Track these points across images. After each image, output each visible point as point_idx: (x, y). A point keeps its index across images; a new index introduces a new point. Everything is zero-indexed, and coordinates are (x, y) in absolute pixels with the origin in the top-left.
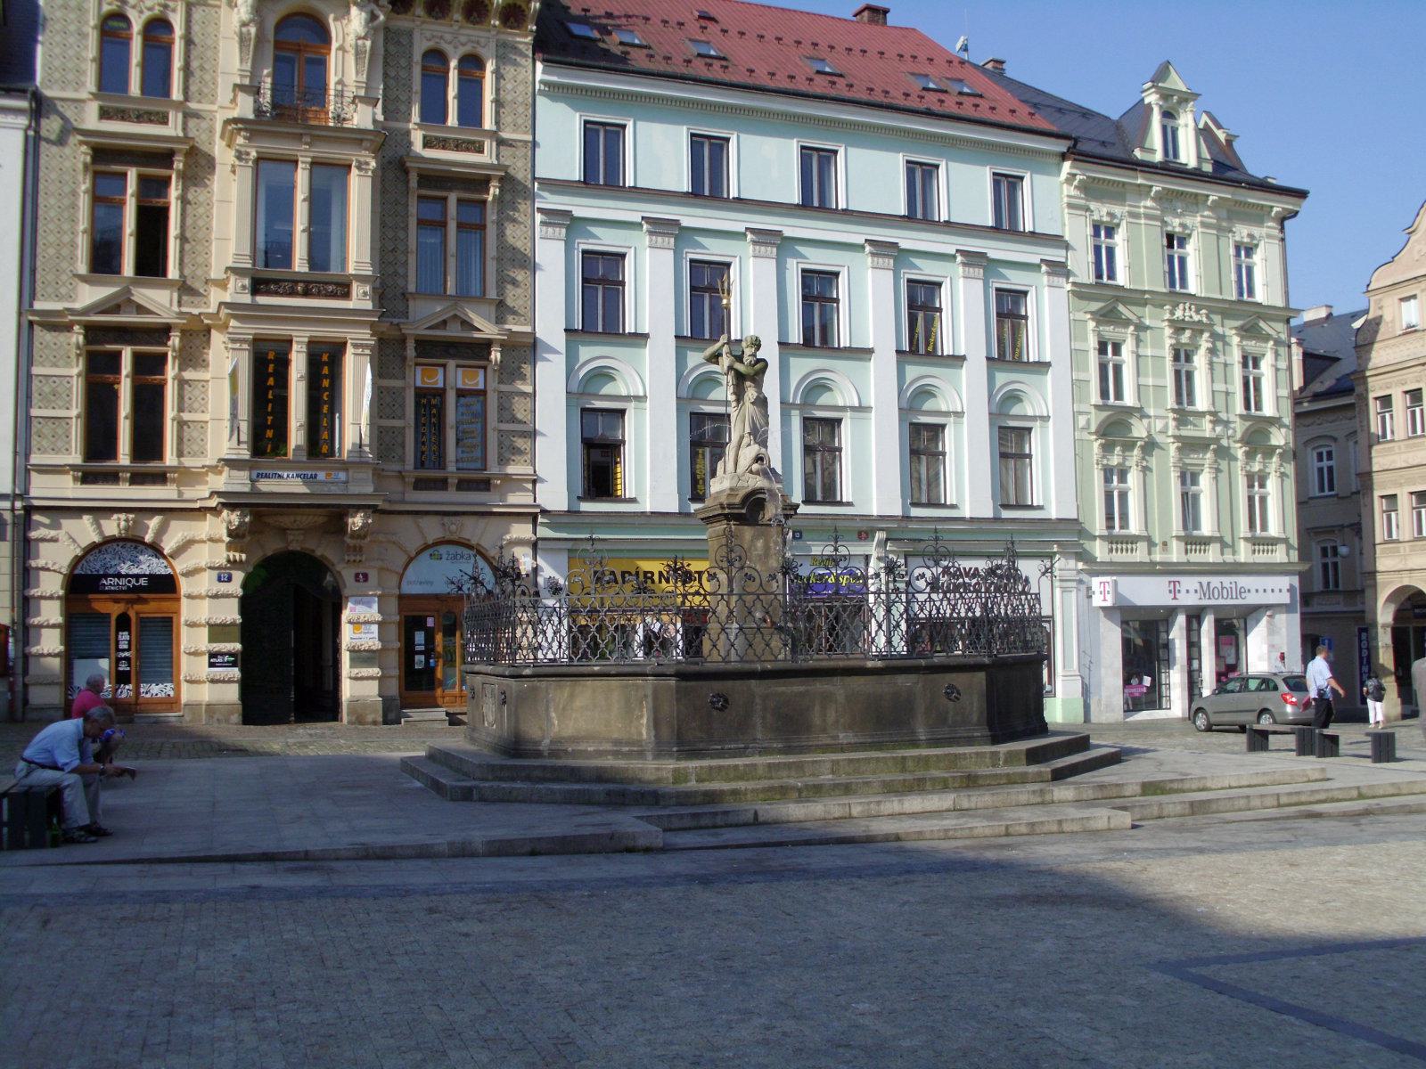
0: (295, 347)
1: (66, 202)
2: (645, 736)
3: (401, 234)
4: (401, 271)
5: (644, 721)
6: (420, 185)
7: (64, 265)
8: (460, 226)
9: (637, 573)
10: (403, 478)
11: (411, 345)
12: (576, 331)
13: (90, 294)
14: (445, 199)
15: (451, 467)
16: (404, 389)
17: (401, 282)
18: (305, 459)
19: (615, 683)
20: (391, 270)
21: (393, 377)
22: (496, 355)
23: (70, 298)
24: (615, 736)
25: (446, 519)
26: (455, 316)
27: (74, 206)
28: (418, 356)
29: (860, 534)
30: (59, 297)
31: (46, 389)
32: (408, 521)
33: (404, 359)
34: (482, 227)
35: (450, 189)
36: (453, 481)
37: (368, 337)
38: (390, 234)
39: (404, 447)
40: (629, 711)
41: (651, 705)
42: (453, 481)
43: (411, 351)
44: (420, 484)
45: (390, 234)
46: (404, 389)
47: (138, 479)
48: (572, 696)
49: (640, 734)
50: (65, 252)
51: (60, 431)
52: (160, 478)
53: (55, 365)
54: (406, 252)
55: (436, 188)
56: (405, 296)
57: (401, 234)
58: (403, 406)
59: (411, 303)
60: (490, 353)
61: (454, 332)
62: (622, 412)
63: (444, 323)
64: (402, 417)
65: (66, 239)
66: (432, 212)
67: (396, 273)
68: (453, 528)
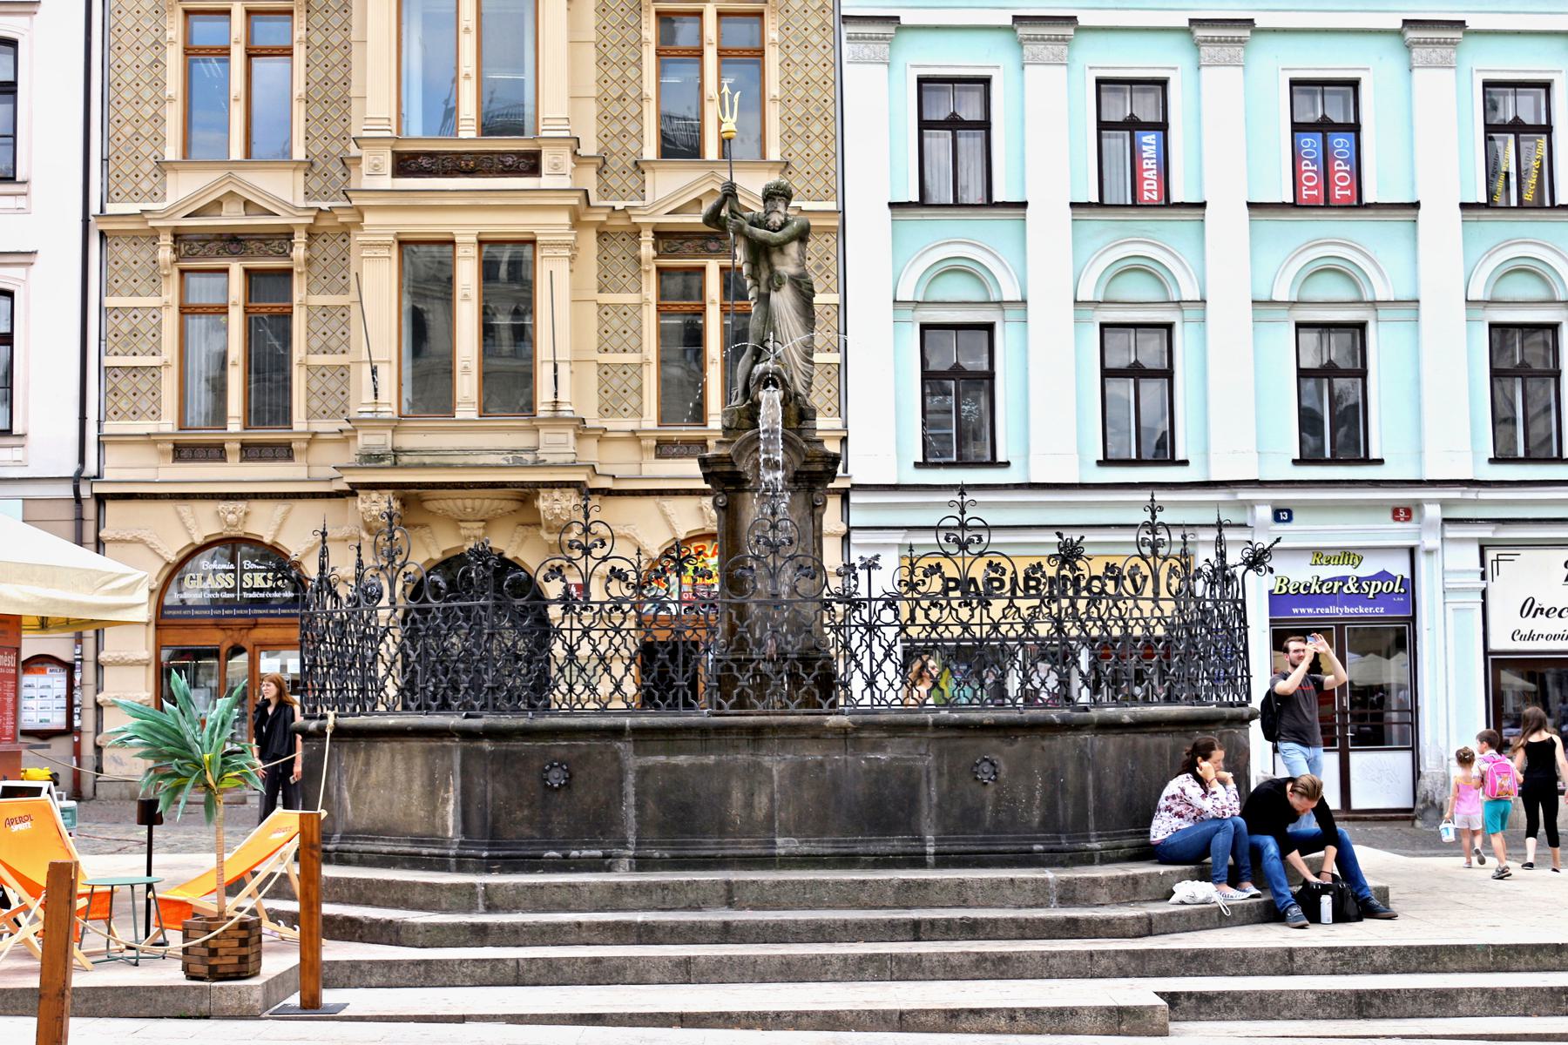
0: (460, 251)
1: (147, 58)
2: (450, 834)
3: (632, 73)
4: (633, 128)
5: (450, 807)
7: (146, 149)
8: (722, 53)
10: (639, 439)
11: (647, 239)
13: (184, 188)
16: (640, 305)
17: (633, 146)
18: (474, 416)
19: (416, 745)
20: (616, 128)
23: (154, 195)
24: (417, 830)
28: (659, 256)
29: (1396, 512)
30: (136, 195)
31: (125, 328)
32: (649, 503)
33: (639, 261)
34: (760, 53)
38: (615, 73)
39: (641, 395)
40: (433, 791)
41: (458, 781)
43: (647, 249)
45: (615, 73)
46: (640, 305)
47: (250, 452)
48: (367, 763)
49: (446, 830)
50: (146, 130)
51: (144, 387)
52: (284, 451)
53: (135, 293)
57: (632, 73)
58: (638, 333)
59: (648, 176)
64: (639, 348)
65: (148, 111)
67: (624, 133)
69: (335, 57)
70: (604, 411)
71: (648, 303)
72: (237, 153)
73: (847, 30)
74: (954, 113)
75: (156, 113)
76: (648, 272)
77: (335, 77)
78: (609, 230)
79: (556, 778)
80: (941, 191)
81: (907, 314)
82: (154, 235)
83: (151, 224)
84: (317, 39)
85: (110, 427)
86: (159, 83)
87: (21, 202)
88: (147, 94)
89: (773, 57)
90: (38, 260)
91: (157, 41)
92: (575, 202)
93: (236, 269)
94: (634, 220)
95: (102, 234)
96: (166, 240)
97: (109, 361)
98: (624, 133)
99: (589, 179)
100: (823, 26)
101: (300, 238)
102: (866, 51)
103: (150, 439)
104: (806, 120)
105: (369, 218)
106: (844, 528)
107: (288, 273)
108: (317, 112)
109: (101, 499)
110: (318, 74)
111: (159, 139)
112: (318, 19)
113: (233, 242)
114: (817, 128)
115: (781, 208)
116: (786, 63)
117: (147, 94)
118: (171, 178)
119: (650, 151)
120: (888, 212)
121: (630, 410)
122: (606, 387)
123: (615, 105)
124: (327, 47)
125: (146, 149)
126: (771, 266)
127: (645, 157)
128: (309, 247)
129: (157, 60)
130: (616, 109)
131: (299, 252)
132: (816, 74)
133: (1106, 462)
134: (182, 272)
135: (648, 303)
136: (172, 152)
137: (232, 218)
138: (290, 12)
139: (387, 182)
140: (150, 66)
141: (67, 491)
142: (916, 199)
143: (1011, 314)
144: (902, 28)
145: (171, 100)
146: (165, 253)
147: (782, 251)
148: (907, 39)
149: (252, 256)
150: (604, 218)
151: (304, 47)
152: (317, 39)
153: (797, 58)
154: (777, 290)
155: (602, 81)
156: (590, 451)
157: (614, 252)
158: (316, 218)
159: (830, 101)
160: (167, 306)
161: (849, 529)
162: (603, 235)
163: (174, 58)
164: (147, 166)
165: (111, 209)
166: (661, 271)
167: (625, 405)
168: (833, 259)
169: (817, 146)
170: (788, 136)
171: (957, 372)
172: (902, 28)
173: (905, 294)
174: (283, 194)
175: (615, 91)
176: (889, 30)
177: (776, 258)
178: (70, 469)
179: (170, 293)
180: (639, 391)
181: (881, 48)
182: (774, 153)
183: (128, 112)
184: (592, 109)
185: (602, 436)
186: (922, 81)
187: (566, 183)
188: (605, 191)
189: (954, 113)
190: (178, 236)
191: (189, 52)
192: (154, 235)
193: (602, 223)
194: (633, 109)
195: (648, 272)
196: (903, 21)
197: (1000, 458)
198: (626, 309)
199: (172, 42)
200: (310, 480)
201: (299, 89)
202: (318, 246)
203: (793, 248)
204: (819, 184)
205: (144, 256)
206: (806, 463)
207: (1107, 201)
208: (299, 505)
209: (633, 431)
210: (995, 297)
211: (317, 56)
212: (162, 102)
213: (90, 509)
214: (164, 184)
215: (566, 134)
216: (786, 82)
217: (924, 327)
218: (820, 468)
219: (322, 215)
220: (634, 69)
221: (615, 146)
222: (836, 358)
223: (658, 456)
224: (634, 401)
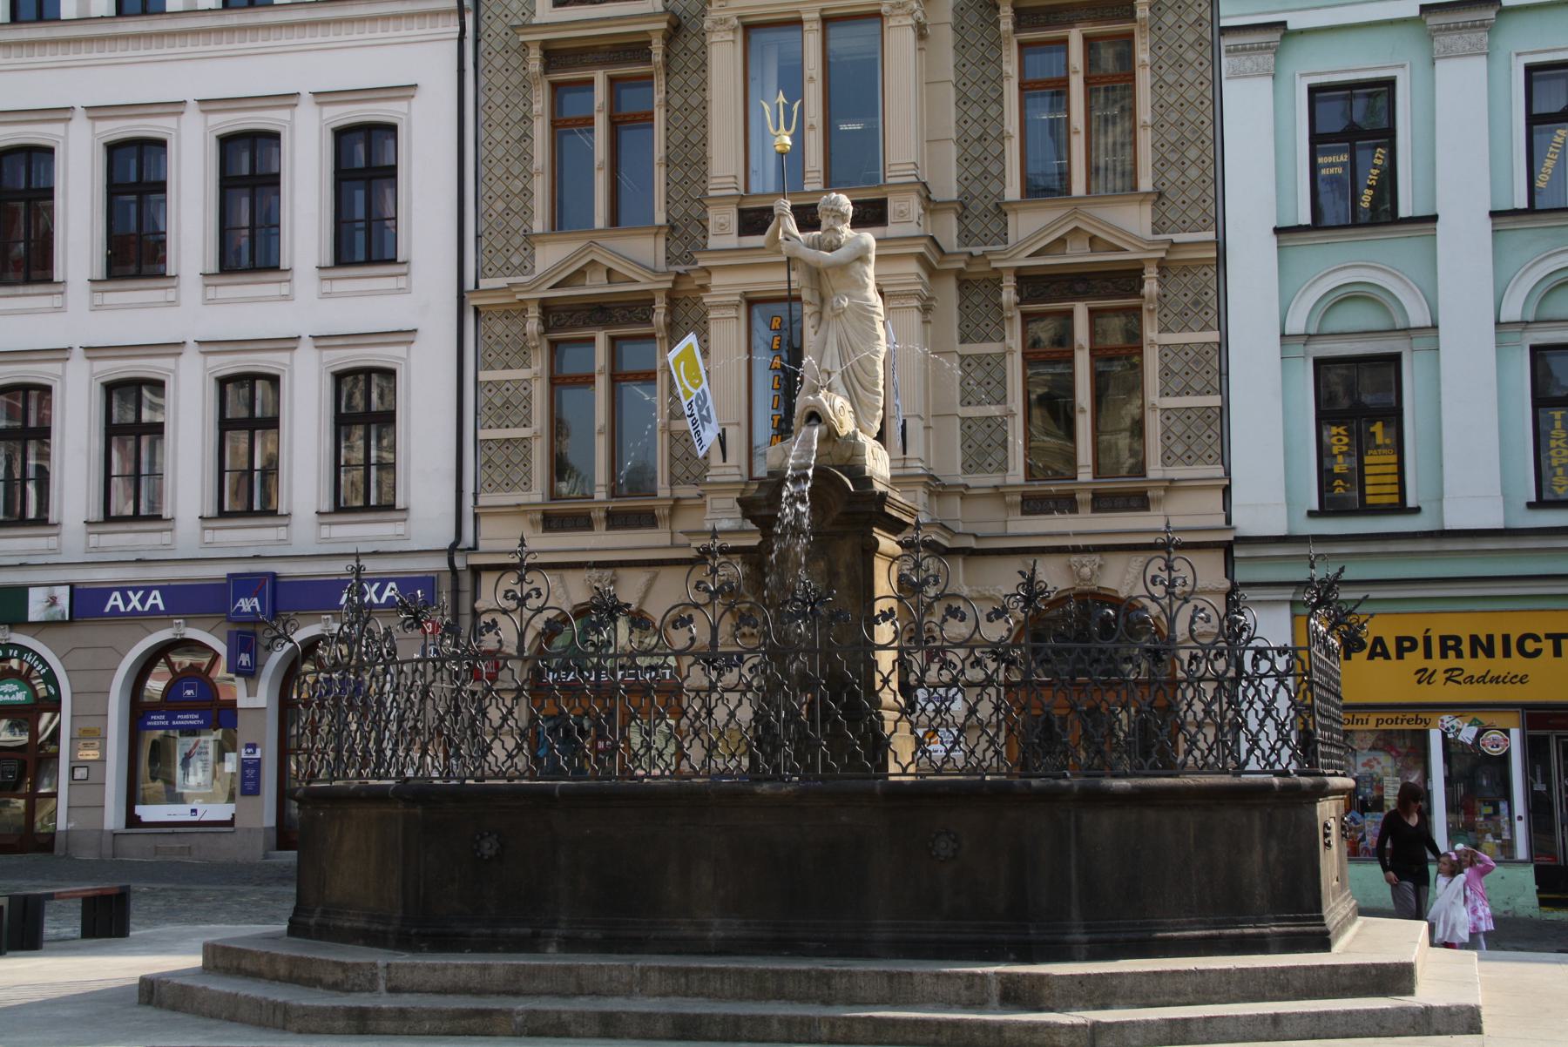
1: (516, 133)
4: (994, 169)
6: (1019, 26)
7: (516, 223)
9: (1427, 640)
10: (1003, 495)
14: (1065, 41)
15: (1085, 475)
16: (1003, 356)
17: (994, 187)
21: (986, 338)
22: (1151, 287)
23: (523, 269)
25: (1074, 558)
26: (1076, 229)
27: (526, 137)
28: (1022, 301)
30: (509, 269)
31: (498, 402)
35: (1070, 24)
36: (1084, 497)
37: (913, 279)
38: (976, 113)
39: (1006, 448)
42: (1084, 497)
43: (1009, 295)
44: (1033, 504)
45: (976, 113)
46: (1003, 356)
47: (616, 520)
50: (516, 204)
51: (516, 460)
52: (646, 519)
54: (1001, 138)
55: (1048, 25)
56: (1001, 210)
58: (1002, 383)
59: (1011, 219)
60: (1141, 285)
61: (1077, 255)
62: (1395, 359)
63: (1061, 241)
64: (1002, 400)
65: (518, 185)
66: (1044, 67)
67: (985, 173)
68: (1086, 571)
69: (694, 119)
70: (967, 468)
71: (1011, 352)
73: (1226, 42)
74: (1355, 130)
75: (525, 188)
76: (1011, 318)
77: (694, 138)
78: (970, 277)
79: (488, 847)
81: (1298, 349)
82: (521, 309)
83: (519, 297)
84: (677, 101)
85: (484, 500)
86: (526, 157)
87: (402, 282)
89: (1144, 79)
90: (419, 338)
91: (525, 116)
92: (922, 249)
93: (601, 338)
94: (994, 265)
95: (477, 310)
96: (534, 313)
97: (483, 434)
98: (985, 173)
99: (948, 230)
100: (1200, 41)
102: (1248, 64)
103: (519, 510)
104: (1180, 145)
105: (717, 280)
106: (1227, 584)
107: (652, 337)
108: (678, 175)
109: (477, 571)
110: (678, 137)
111: (527, 212)
112: (677, 81)
113: (600, 311)
114: (1193, 153)
116: (1158, 84)
119: (1013, 191)
121: (995, 465)
122: (969, 442)
123: (978, 145)
125: (516, 223)
127: (1008, 198)
129: (525, 134)
130: (977, 150)
131: (659, 317)
132: (1191, 94)
133: (1540, 503)
134: (554, 344)
135: (1011, 352)
136: (539, 225)
137: (595, 286)
138: (651, 76)
139: (733, 240)
140: (519, 141)
141: (441, 564)
143: (1419, 342)
146: (533, 325)
149: (617, 325)
150: (962, 265)
151: (663, 110)
152: (677, 101)
153: (1170, 79)
155: (961, 122)
156: (955, 510)
157: (976, 300)
158: (675, 282)
159: (1207, 122)
160: (536, 377)
161: (1234, 588)
162: (965, 283)
163: (541, 131)
164: (517, 240)
165: (484, 284)
166: (1027, 318)
167: (990, 460)
168: (1211, 293)
169: (1193, 173)
170: (1161, 164)
174: (640, 258)
175: (975, 132)
176: (1275, 37)
178: (445, 538)
179: (539, 364)
180: (1004, 444)
182: (1145, 184)
183: (499, 188)
184: (953, 151)
185: (964, 493)
187: (913, 230)
188: (965, 236)
189: (1355, 130)
190: (546, 307)
193: (960, 271)
194: (994, 149)
195: (1011, 318)
196: (1291, 26)
197: (1411, 503)
198: (989, 359)
200: (673, 546)
201: (659, 152)
204: (1195, 214)
205: (515, 329)
207: (1538, 206)
208: (665, 572)
209: (996, 487)
210: (1400, 324)
211: (676, 119)
212: (530, 176)
213: (466, 582)
214: (533, 256)
215: (913, 179)
216: (1159, 106)
220: (995, 107)
221: (976, 189)
222: (1215, 400)
223: (1024, 513)
224: (999, 456)
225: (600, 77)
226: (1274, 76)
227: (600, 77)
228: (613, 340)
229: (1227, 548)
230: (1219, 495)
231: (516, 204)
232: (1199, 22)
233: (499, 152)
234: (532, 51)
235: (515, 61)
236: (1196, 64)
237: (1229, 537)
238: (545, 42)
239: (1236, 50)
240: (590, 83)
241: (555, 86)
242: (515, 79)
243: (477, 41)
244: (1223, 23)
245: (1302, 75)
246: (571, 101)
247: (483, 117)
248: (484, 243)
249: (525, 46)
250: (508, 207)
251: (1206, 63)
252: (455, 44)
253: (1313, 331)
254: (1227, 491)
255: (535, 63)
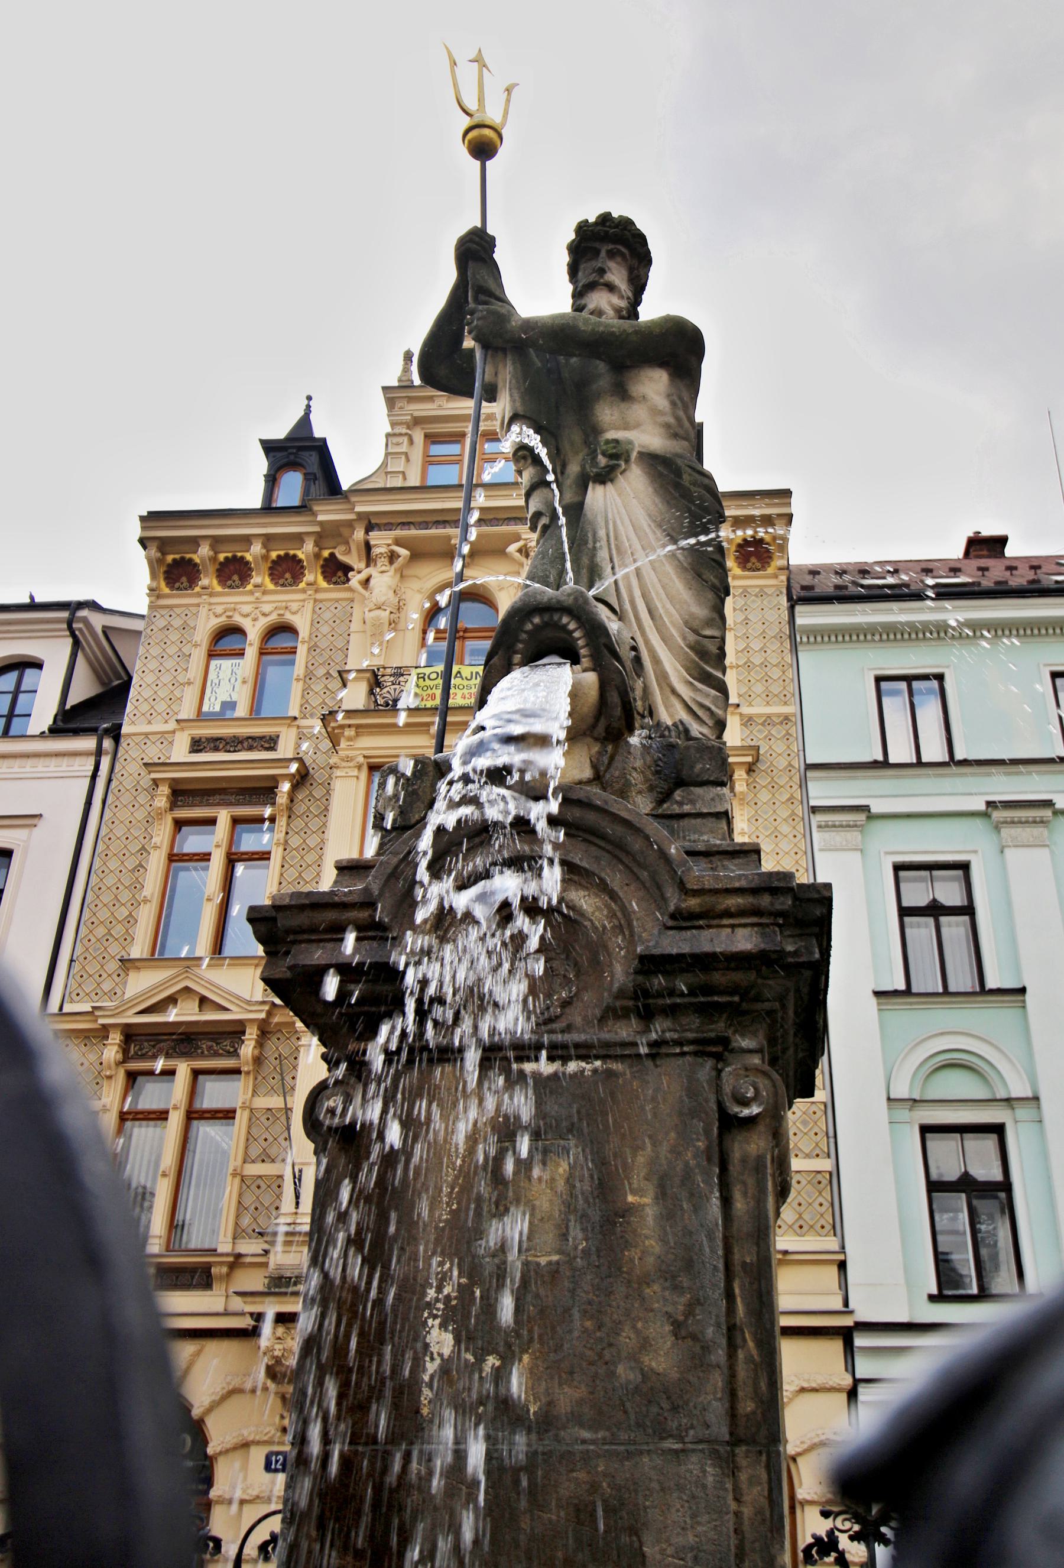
1: (131, 863)
12: (896, 993)
13: (142, 984)
50: (118, 930)
69: (310, 858)
72: (203, 946)
73: (817, 819)
80: (927, 980)
81: (903, 1114)
82: (104, 1032)
84: (295, 841)
86: (137, 886)
88: (125, 896)
96: (116, 1038)
100: (793, 815)
101: (251, 1034)
106: (847, 1381)
111: (128, 938)
112: (298, 823)
115: (617, 275)
117: (125, 896)
118: (133, 976)
120: (874, 1000)
124: (305, 848)
126: (592, 431)
128: (260, 1044)
136: (139, 950)
140: (133, 871)
142: (902, 986)
144: (872, 817)
145: (146, 901)
147: (622, 393)
148: (878, 826)
151: (281, 848)
154: (605, 477)
161: (857, 1382)
163: (156, 862)
171: (966, 1184)
172: (872, 817)
173: (901, 1090)
176: (861, 817)
177: (607, 413)
181: (854, 836)
183: (103, 914)
186: (898, 868)
191: (174, 858)
192: (104, 1032)
196: (874, 810)
199: (156, 847)
202: (271, 1045)
203: (654, 385)
206: (682, 920)
210: (1001, 1094)
212: (136, 904)
217: (926, 1130)
218: (744, 940)
219: (275, 1011)
222: (827, 1165)
225: (224, 816)
226: (861, 851)
227: (224, 816)
228: (196, 1073)
229: (846, 1335)
230: (834, 1270)
231: (118, 930)
232: (791, 800)
233: (110, 881)
234: (161, 788)
235: (143, 798)
236: (791, 836)
237: (848, 1321)
238: (174, 779)
239: (827, 826)
240: (212, 822)
241: (179, 824)
242: (141, 814)
243: (110, 781)
244: (812, 803)
245: (887, 853)
246: (193, 842)
247: (101, 847)
248: (77, 967)
249: (156, 782)
250: (109, 933)
251: (799, 836)
252: (88, 780)
253: (917, 1097)
254: (842, 1266)
255: (162, 801)
